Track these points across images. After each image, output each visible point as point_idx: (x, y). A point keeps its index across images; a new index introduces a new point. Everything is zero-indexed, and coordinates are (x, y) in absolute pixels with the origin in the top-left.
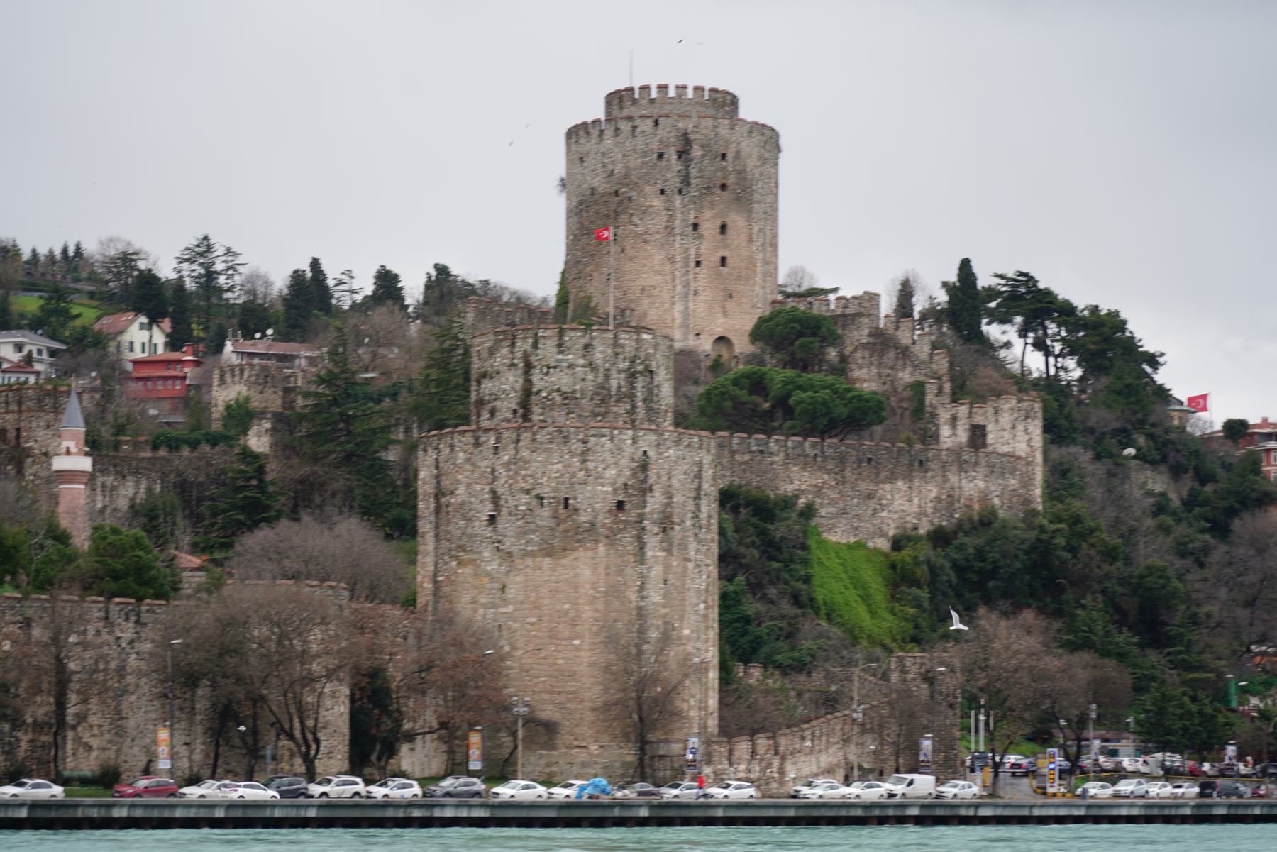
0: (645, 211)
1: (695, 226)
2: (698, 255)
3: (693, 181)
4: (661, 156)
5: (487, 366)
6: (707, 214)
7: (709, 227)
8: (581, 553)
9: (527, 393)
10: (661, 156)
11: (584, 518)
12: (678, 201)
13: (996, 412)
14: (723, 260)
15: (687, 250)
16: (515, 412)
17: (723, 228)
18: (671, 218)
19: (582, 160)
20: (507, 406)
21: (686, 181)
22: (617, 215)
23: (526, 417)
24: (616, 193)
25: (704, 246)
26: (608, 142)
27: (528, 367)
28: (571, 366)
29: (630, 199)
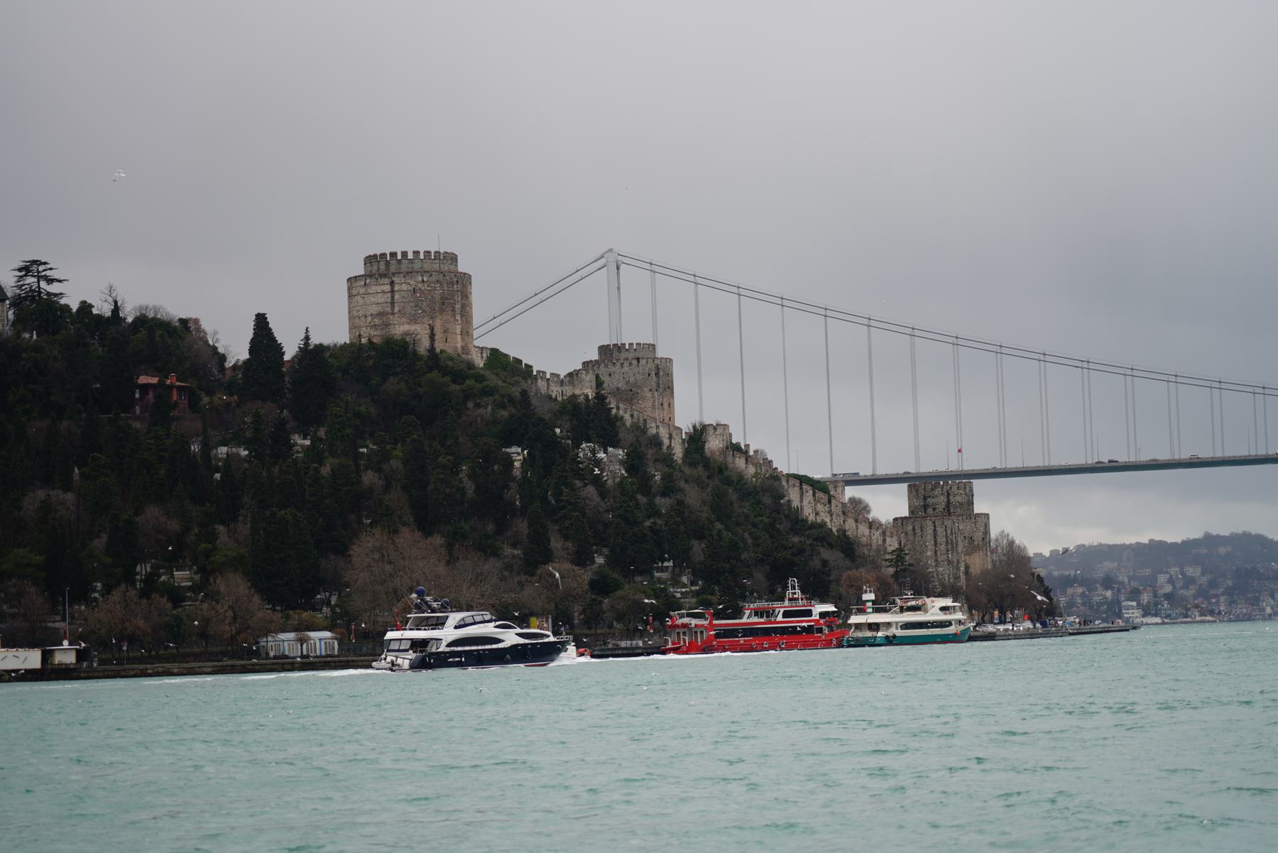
0: (644, 398)
1: (662, 404)
2: (663, 417)
3: (661, 386)
4: (649, 375)
5: (931, 493)
6: (665, 399)
7: (666, 405)
8: (977, 554)
9: (948, 503)
10: (649, 375)
11: (976, 543)
12: (656, 393)
13: (835, 487)
14: (670, 418)
15: (660, 415)
16: (944, 509)
17: (669, 404)
18: (654, 401)
19: (610, 375)
20: (940, 508)
21: (658, 386)
22: (631, 400)
23: (949, 511)
24: (631, 390)
25: (665, 413)
26: (626, 368)
27: (948, 494)
28: (961, 494)
29: (638, 393)
